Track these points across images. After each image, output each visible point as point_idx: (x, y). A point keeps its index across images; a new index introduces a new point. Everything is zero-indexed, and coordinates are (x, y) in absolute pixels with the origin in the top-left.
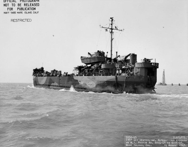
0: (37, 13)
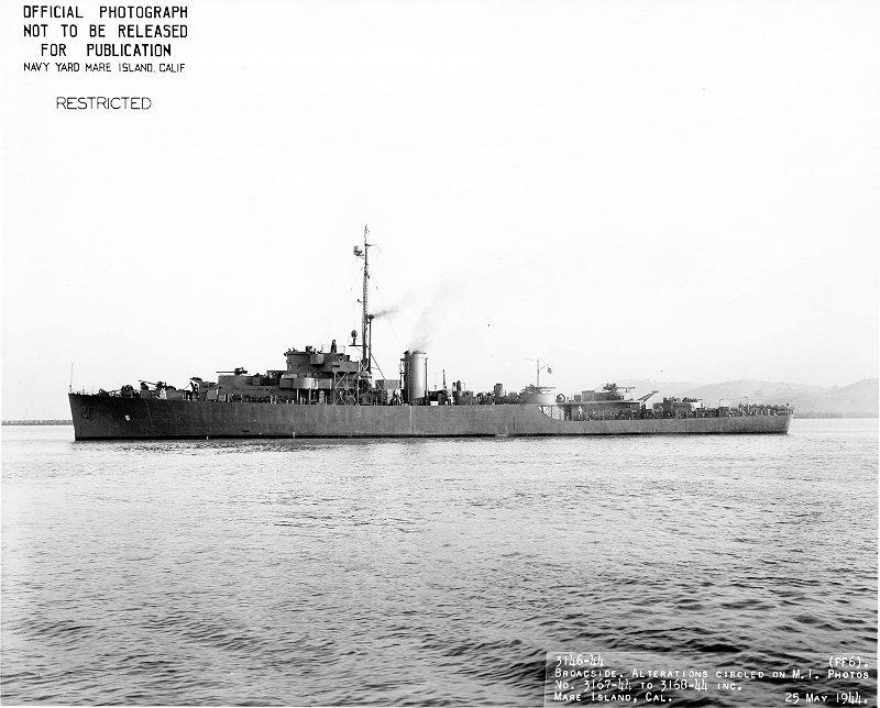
0: (175, 69)
